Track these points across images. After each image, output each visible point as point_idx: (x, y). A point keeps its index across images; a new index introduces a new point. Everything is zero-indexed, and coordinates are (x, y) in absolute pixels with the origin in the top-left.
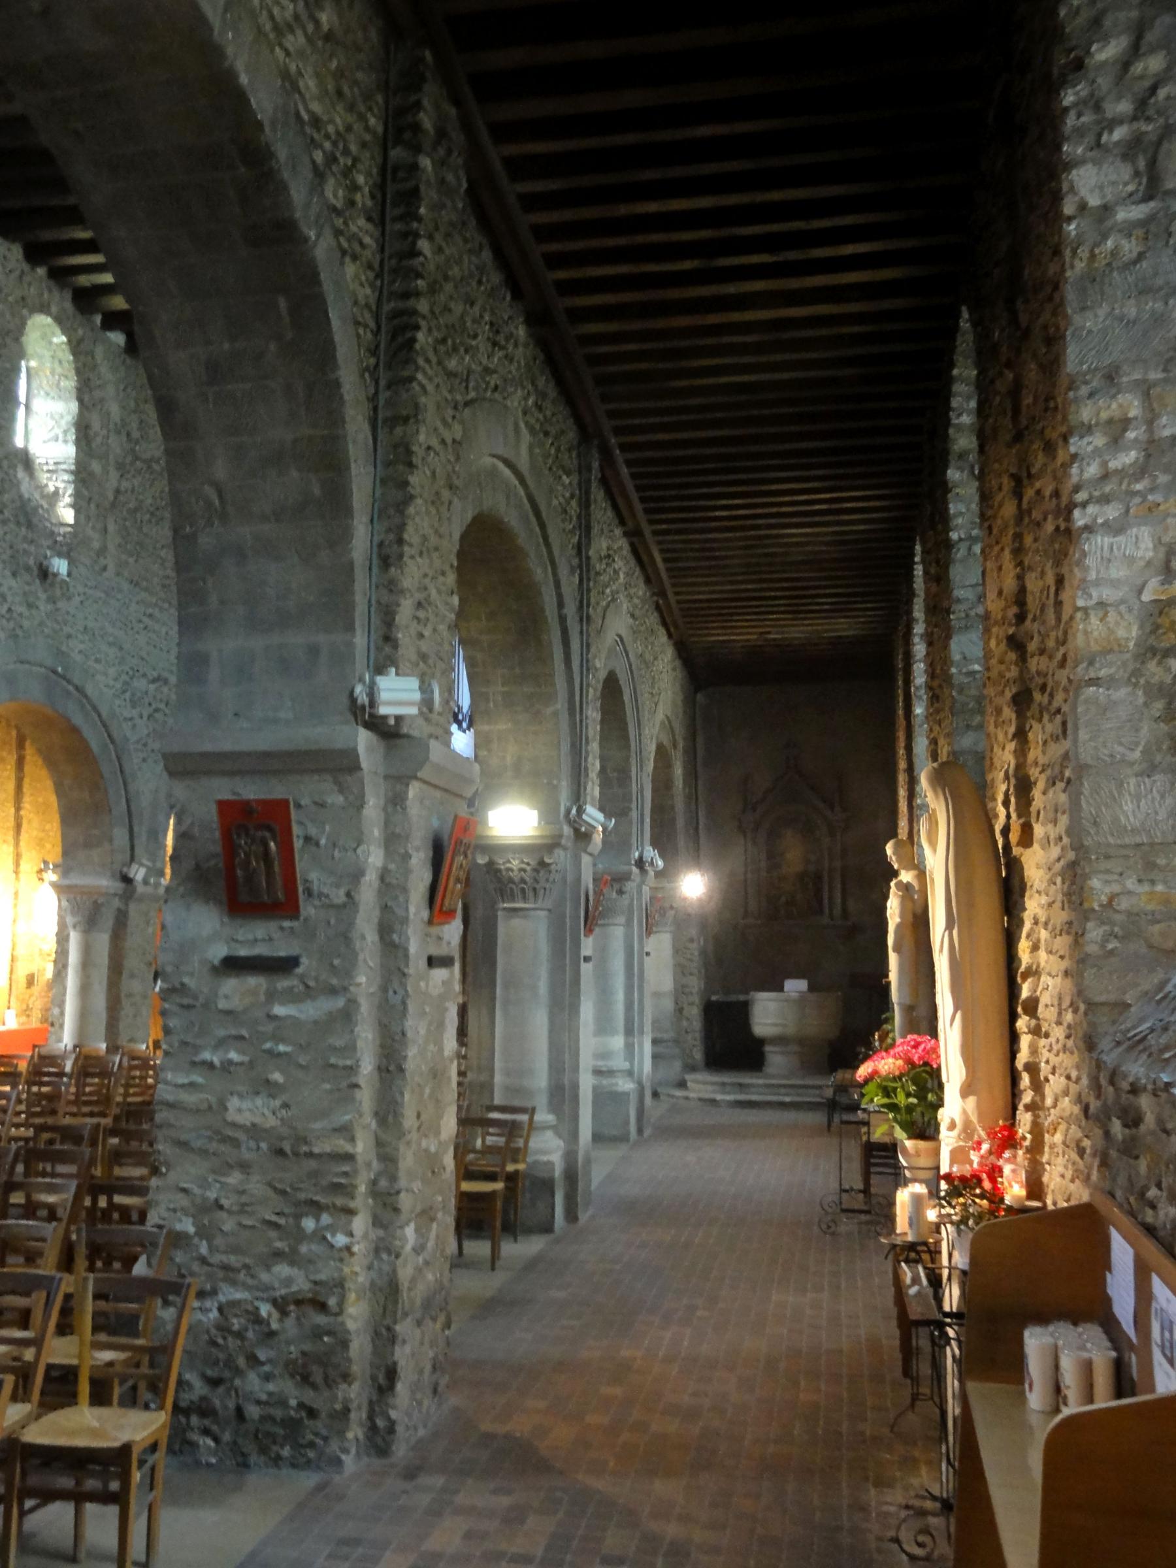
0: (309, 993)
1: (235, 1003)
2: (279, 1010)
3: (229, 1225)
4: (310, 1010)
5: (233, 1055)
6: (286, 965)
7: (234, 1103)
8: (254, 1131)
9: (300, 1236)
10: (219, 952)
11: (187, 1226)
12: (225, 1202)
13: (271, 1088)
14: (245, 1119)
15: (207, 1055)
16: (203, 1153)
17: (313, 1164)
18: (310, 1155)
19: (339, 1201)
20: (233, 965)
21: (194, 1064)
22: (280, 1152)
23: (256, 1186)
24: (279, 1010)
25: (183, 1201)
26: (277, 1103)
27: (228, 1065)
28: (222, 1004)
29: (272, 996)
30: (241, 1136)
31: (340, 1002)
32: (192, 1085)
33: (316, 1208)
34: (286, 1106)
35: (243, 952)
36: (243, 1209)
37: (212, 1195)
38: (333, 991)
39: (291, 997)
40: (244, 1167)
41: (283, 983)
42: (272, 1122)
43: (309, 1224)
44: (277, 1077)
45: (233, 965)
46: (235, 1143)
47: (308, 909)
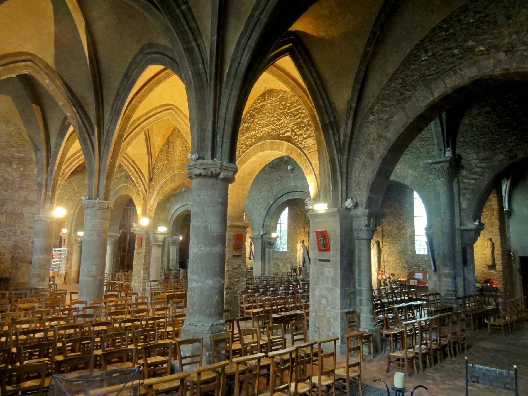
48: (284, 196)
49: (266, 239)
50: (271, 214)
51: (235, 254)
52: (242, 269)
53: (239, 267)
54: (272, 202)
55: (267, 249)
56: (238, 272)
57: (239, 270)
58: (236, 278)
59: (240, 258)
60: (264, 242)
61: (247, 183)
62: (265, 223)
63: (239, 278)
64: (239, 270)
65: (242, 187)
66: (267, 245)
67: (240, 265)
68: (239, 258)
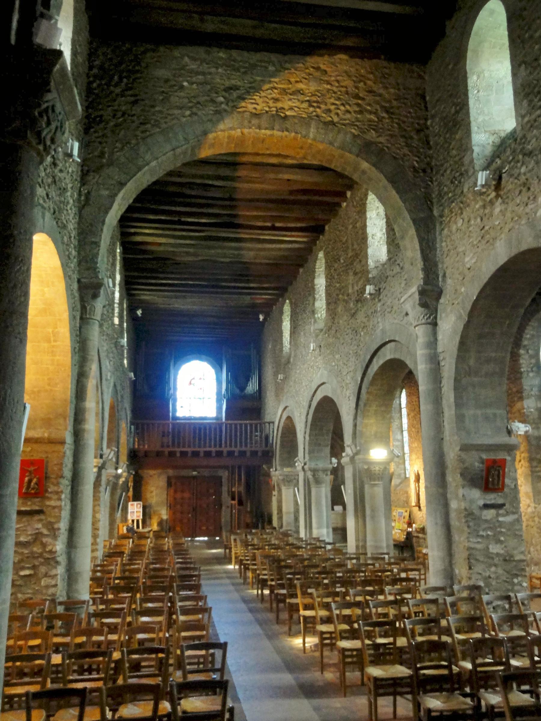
0: (507, 514)
1: (489, 517)
2: (501, 519)
3: (494, 583)
4: (510, 519)
5: (489, 533)
6: (501, 506)
7: (491, 547)
8: (498, 554)
9: (513, 584)
10: (481, 503)
11: (482, 584)
12: (492, 576)
13: (501, 542)
14: (495, 551)
15: (481, 533)
16: (482, 562)
17: (514, 563)
18: (514, 561)
19: (523, 573)
20: (486, 506)
21: (478, 536)
22: (505, 560)
23: (500, 571)
24: (501, 519)
25: (480, 577)
26: (503, 546)
27: (488, 535)
28: (483, 518)
29: (498, 515)
30: (493, 556)
31: (516, 516)
32: (478, 542)
33: (517, 576)
34: (505, 547)
35: (488, 502)
36: (497, 578)
37: (487, 574)
38: (514, 513)
39: (503, 516)
40: (496, 565)
41: (501, 511)
42: (502, 552)
43: (516, 581)
44: (502, 538)
45: (486, 506)
46: (493, 558)
47: (506, 490)
48: (375, 360)
49: (360, 465)
50: (361, 403)
51: (23, 509)
52: (44, 545)
53: (35, 540)
54: (359, 379)
55: (366, 487)
56: (32, 553)
57: (37, 549)
58: (23, 568)
59: (42, 517)
60: (360, 472)
61: (55, 334)
62: (358, 428)
63: (34, 567)
64: (37, 549)
65: (46, 345)
66: (365, 479)
67: (37, 536)
68: (37, 517)
